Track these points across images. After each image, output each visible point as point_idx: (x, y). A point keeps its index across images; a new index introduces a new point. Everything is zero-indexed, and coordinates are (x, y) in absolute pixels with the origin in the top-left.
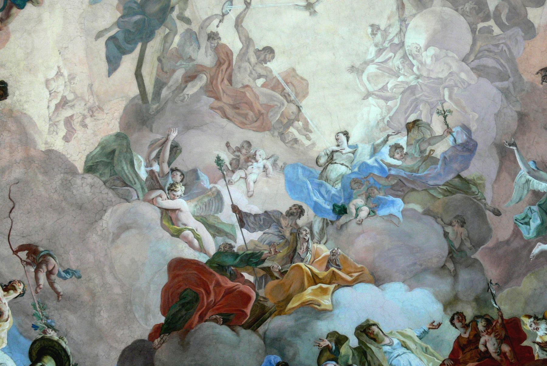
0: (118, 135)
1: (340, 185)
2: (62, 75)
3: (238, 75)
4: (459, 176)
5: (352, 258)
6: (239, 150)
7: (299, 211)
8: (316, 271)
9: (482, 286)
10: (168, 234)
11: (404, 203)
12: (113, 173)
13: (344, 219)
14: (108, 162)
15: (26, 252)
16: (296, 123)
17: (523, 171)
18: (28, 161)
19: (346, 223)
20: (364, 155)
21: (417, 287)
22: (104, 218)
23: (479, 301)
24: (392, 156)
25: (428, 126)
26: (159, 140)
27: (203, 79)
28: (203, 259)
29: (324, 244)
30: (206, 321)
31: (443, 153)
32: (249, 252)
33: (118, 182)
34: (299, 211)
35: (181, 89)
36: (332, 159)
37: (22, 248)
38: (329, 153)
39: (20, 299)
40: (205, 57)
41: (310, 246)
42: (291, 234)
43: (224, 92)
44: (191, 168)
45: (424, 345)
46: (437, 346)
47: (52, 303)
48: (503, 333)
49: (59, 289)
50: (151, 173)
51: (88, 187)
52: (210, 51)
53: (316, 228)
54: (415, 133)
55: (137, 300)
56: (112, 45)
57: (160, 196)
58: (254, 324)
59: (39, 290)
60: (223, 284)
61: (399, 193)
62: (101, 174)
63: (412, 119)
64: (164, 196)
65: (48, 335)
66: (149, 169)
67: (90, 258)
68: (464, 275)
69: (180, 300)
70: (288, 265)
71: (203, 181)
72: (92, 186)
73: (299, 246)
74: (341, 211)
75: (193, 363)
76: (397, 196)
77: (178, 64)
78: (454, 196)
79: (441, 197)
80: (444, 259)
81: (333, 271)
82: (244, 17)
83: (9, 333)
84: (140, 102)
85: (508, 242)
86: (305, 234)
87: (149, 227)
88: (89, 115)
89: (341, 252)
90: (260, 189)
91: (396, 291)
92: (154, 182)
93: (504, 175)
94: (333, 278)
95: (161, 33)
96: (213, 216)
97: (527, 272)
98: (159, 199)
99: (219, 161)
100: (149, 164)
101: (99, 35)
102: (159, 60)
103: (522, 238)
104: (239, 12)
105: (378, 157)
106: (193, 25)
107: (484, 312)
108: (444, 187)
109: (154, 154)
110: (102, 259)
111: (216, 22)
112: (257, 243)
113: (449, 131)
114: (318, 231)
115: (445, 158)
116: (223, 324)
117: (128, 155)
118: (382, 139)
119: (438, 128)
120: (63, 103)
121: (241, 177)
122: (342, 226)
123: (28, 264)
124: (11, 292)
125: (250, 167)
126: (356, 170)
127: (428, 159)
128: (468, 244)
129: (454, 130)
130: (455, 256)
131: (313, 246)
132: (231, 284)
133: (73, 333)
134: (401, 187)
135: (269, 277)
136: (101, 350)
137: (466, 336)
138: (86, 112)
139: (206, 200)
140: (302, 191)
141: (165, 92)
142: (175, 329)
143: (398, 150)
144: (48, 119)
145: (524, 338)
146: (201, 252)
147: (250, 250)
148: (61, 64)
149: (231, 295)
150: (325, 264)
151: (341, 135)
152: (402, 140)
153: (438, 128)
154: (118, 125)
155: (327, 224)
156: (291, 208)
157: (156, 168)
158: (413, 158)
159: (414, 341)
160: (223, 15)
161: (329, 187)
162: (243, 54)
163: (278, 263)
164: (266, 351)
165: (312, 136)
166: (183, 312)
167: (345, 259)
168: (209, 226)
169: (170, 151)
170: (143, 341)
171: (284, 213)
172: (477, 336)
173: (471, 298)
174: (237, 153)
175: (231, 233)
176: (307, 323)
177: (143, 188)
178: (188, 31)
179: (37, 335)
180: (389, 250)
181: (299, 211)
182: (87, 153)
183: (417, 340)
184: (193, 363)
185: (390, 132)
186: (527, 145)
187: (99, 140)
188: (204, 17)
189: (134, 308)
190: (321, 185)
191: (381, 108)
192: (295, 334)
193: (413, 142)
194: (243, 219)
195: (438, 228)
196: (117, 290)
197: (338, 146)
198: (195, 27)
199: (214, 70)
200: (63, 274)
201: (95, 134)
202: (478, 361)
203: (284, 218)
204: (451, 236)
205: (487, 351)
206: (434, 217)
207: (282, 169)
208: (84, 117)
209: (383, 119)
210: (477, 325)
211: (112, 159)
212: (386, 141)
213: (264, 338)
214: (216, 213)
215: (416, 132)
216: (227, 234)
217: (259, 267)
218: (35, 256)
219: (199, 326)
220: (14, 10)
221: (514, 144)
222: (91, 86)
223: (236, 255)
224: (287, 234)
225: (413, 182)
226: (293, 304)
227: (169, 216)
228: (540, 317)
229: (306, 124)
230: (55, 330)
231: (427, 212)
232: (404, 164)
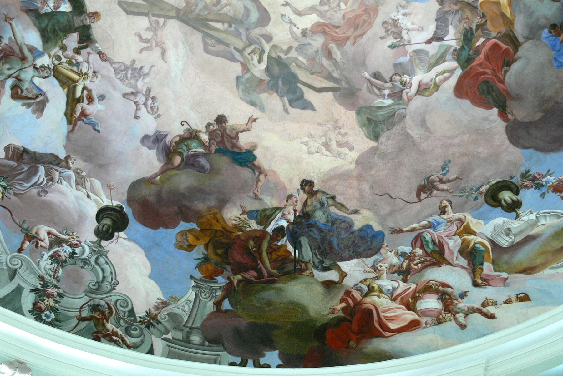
0: (358, 113)
2: (307, 142)
3: (334, 21)
6: (387, 31)
12: (383, 122)
14: (375, 124)
15: (422, 193)
18: (360, 177)
22: (412, 135)
26: (368, 86)
27: (333, 46)
28: (459, 72)
30: (504, 79)
32: (462, 38)
33: (390, 120)
35: (335, 63)
37: (418, 195)
39: (453, 205)
40: (318, 42)
42: (456, 5)
43: (344, 33)
44: (392, 67)
47: (462, 184)
49: (454, 177)
50: (390, 96)
51: (388, 142)
52: (315, 37)
56: (295, 104)
58: (515, 44)
59: (451, 191)
60: (480, 62)
62: (382, 131)
64: (408, 90)
65: (484, 191)
66: (386, 97)
67: (438, 151)
70: (478, 11)
72: (388, 139)
75: (533, 94)
77: (318, 61)
82: (295, 9)
83: (474, 217)
84: (338, 93)
88: (339, 130)
92: (397, 95)
95: (294, 69)
96: (430, 58)
98: (409, 94)
99: (392, 47)
100: (383, 96)
101: (286, 111)
102: (312, 74)
104: (291, 12)
106: (293, 45)
109: (377, 91)
110: (441, 143)
111: (294, 29)
120: (327, 145)
121: (407, 33)
123: (430, 194)
124: (446, 209)
125: (401, 25)
132: (482, 56)
133: (488, 174)
135: (484, 27)
136: (505, 157)
138: (337, 132)
139: (417, 61)
141: (336, 75)
142: (504, 102)
144: (334, 158)
148: (300, 141)
149: (490, 57)
154: (350, 112)
157: (387, 92)
160: (291, 23)
162: (321, 14)
163: (475, 18)
164: (537, 39)
166: (494, 94)
168: (437, 63)
170: (507, 127)
171: (440, 7)
174: (390, 31)
176: (525, 5)
177: (399, 104)
178: (297, 50)
179: (482, 199)
182: (365, 137)
188: (290, 36)
192: (530, 15)
194: (437, 38)
196: (466, 137)
198: (295, 44)
199: (327, 37)
200: (444, 172)
201: (353, 129)
203: (444, 8)
208: (339, 133)
211: (373, 121)
213: (527, 39)
214: (428, 56)
216: (446, 52)
218: (426, 188)
220: (256, 163)
222: (319, 124)
223: (462, 48)
224: (455, 7)
226: (508, 13)
227: (422, 90)
230: (482, 186)
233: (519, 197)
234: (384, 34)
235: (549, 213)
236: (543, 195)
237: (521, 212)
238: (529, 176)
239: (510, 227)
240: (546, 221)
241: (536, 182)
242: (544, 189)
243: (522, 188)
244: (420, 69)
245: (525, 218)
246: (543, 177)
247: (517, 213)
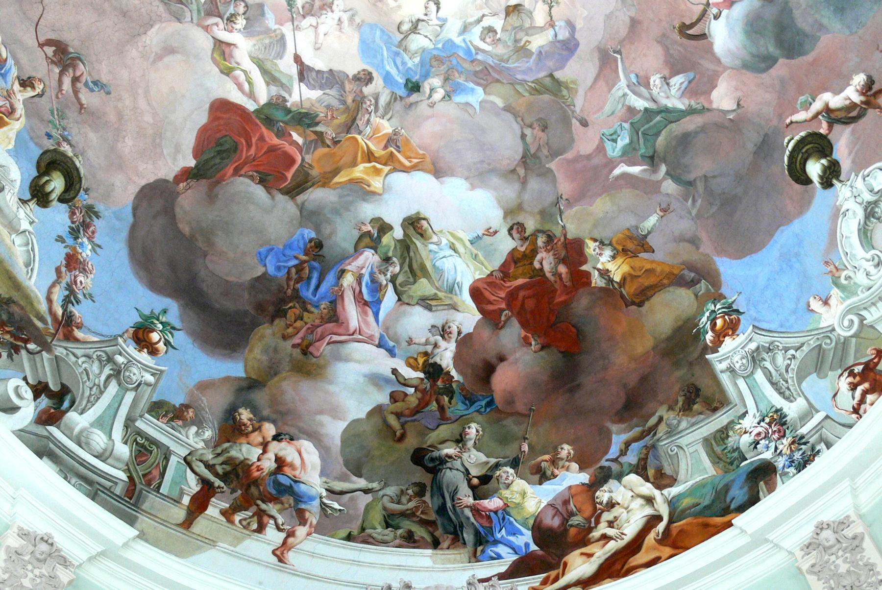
1: (419, 58)
4: (551, 76)
5: (415, 141)
7: (368, 78)
8: (372, 147)
9: (551, 199)
13: (415, 97)
15: (54, 48)
17: (623, 82)
20: (452, 32)
21: (480, 187)
22: (149, 33)
23: (544, 214)
24: (483, 39)
25: (530, 14)
28: (251, 106)
30: (241, 176)
32: (304, 111)
34: (368, 78)
36: (416, 28)
37: (49, 43)
38: (414, 20)
39: (36, 99)
41: (372, 120)
46: (488, 254)
47: (72, 114)
48: (563, 253)
49: (84, 101)
53: (383, 101)
54: (514, 20)
55: (169, 134)
57: (217, 24)
58: (294, 190)
59: (60, 96)
60: (267, 139)
61: (482, 81)
64: (221, 26)
65: (62, 149)
67: (125, 74)
68: (534, 184)
73: (360, 115)
74: (414, 87)
75: (218, 218)
76: (478, 84)
78: (541, 96)
79: (527, 94)
80: (515, 163)
81: (392, 152)
83: (18, 134)
85: (588, 157)
86: (369, 104)
87: (196, 56)
91: (455, 189)
93: (601, 83)
94: (390, 160)
97: (602, 193)
98: (215, 28)
103: (605, 155)
105: (467, 37)
107: (547, 227)
108: (533, 85)
110: (137, 79)
112: (314, 102)
113: (552, 24)
115: (540, 52)
118: (475, 18)
122: (411, 104)
123: (53, 62)
124: (29, 89)
125: (323, 16)
126: (440, 46)
127: (522, 51)
128: (545, 151)
129: (557, 23)
131: (375, 120)
132: (276, 141)
133: (90, 154)
134: (486, 75)
135: (319, 143)
136: (118, 180)
137: (523, 249)
139: (267, 41)
140: (375, 57)
143: (490, 34)
145: (585, 262)
150: (385, 142)
152: (498, 23)
153: (540, 17)
155: (396, 99)
156: (359, 73)
159: (464, 245)
161: (406, 58)
164: (300, 223)
166: (217, 160)
167: (407, 141)
168: (264, 72)
170: (167, 181)
171: (351, 77)
172: (534, 252)
173: (536, 210)
176: (352, 202)
177: (199, 11)
179: (49, 145)
180: (457, 141)
183: (468, 244)
184: (218, 218)
185: (486, 11)
186: (633, 55)
193: (509, 28)
194: (304, 72)
195: (516, 128)
196: (148, 118)
197: (426, 15)
202: (530, 278)
203: (349, 81)
204: (529, 139)
205: (542, 269)
206: (514, 115)
207: (359, 26)
210: (536, 239)
212: (479, 21)
213: (301, 208)
214: (276, 58)
215: (515, 18)
216: (282, 85)
218: (63, 56)
221: (619, 52)
223: (288, 111)
224: (349, 100)
225: (499, 72)
226: (340, 178)
227: (222, 49)
228: (607, 242)
230: (71, 146)
231: (508, 109)
233: (55, 203)
235: (33, 249)
236: (60, 239)
237: (32, 207)
238: (90, 217)
239: (6, 191)
240: (20, 246)
241: (81, 229)
242: (70, 241)
243: (70, 207)
244: (255, 45)
245: (21, 214)
246: (90, 239)
247: (29, 201)
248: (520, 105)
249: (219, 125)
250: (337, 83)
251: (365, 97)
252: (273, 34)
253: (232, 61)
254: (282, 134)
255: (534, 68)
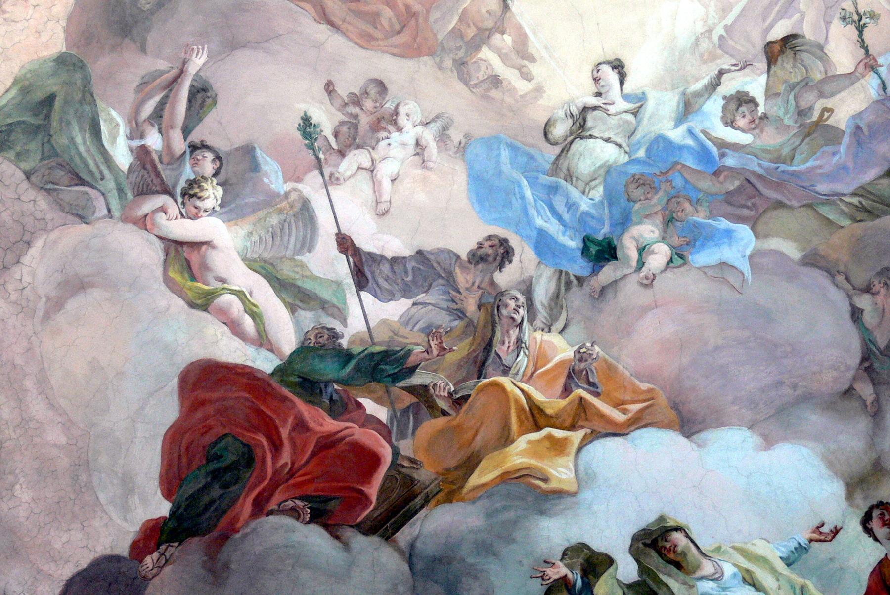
0: (61, 61)
1: (601, 189)
5: (626, 365)
6: (356, 100)
7: (502, 252)
8: (538, 396)
10: (181, 302)
11: (757, 236)
12: (50, 153)
13: (608, 272)
16: (497, 39)
19: (615, 282)
20: (662, 119)
21: (785, 439)
24: (730, 123)
25: (819, 51)
28: (265, 363)
29: (561, 332)
30: (271, 513)
31: (854, 117)
32: (378, 349)
33: (59, 173)
34: (502, 252)
36: (582, 126)
38: (575, 112)
41: (526, 338)
42: (479, 308)
44: (239, 141)
45: (800, 580)
50: (142, 154)
53: (542, 293)
54: (786, 68)
55: (104, 460)
57: (163, 209)
58: (388, 522)
60: (312, 425)
61: (746, 212)
62: (18, 155)
63: (779, 32)
64: (174, 210)
66: (136, 143)
69: (208, 461)
70: (472, 382)
71: (266, 175)
74: (604, 252)
78: (877, 221)
79: (846, 223)
80: (850, 374)
81: (581, 399)
87: (134, 285)
89: (601, 353)
90: (407, 198)
91: (731, 450)
96: (292, 259)
98: (161, 218)
99: (307, 126)
100: (136, 132)
105: (695, 123)
108: (855, 200)
109: (149, 108)
110: (19, 361)
112: (396, 327)
113: (870, 64)
114: (546, 302)
115: (858, 128)
116: (308, 523)
117: (87, 108)
119: (842, 54)
121: (359, 168)
122: (603, 289)
125: (383, 144)
126: (641, 154)
127: (816, 131)
129: (880, 61)
130: (876, 365)
131: (534, 337)
132: (330, 425)
134: (751, 196)
135: (424, 410)
139: (274, 220)
140: (508, 204)
142: (193, 532)
143: (743, 109)
146: (261, 345)
147: (380, 344)
150: (562, 381)
151: (606, 69)
152: (755, 84)
153: (842, 54)
154: (62, 35)
155: (568, 284)
156: (480, 245)
157: (154, 141)
158: (781, 127)
159: (773, 571)
163: (448, 377)
165: (534, 69)
166: (216, 492)
167: (610, 370)
168: (280, 285)
169: (190, 101)
170: (116, 559)
171: (464, 257)
174: (354, 110)
175: (335, 301)
176: (515, 523)
177: (120, 190)
180: (717, 348)
181: (501, 250)
183: (781, 566)
185: (725, 63)
187: (16, 70)
189: (96, 481)
190: (554, 189)
191: (706, 6)
192: (486, 548)
193: (781, 88)
194: (363, 268)
195: (837, 297)
196: (55, 436)
197: (599, 95)
203: (462, 267)
204: (869, 318)
206: (828, 271)
207: (462, 149)
209: (710, 31)
211: (48, 117)
212: (714, 85)
213: (410, 556)
215: (789, 66)
216: (324, 306)
217: (401, 384)
219: (253, 524)
223: (346, 356)
224: (471, 306)
225: (779, 186)
226: (482, 476)
227: (184, 256)
229: (522, 40)
231: (812, 260)
232: (759, 143)
234: (343, 90)
244: (250, 234)
248: (837, 246)
249: (206, 418)
250: (440, 276)
251: (502, 293)
252: (284, 204)
253: (210, 277)
254: (342, 408)
255: (851, 165)
